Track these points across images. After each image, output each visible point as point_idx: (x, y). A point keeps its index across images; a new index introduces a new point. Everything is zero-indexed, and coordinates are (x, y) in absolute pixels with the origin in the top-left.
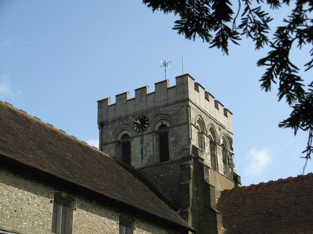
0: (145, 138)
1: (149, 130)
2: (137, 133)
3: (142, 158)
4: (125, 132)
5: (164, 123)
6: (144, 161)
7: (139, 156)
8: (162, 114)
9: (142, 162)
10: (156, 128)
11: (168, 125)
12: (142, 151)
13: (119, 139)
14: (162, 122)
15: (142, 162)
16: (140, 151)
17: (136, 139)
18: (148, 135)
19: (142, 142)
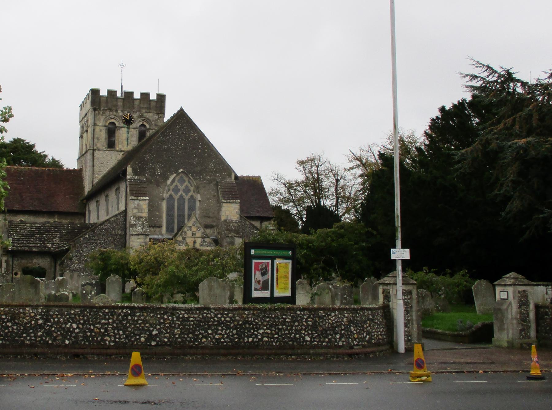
0: (130, 130)
1: (134, 125)
2: (124, 125)
3: (128, 144)
4: (113, 121)
5: (145, 123)
6: (128, 146)
7: (125, 142)
8: (145, 117)
9: (127, 147)
10: (138, 126)
11: (148, 126)
12: (128, 139)
13: (107, 124)
14: (143, 123)
15: (127, 147)
16: (126, 139)
17: (123, 129)
18: (133, 129)
19: (128, 132)
